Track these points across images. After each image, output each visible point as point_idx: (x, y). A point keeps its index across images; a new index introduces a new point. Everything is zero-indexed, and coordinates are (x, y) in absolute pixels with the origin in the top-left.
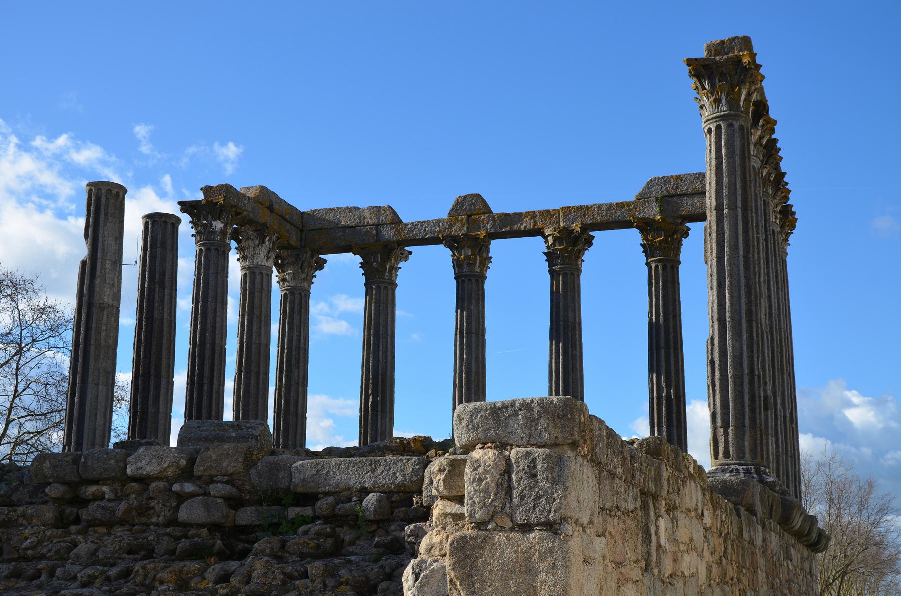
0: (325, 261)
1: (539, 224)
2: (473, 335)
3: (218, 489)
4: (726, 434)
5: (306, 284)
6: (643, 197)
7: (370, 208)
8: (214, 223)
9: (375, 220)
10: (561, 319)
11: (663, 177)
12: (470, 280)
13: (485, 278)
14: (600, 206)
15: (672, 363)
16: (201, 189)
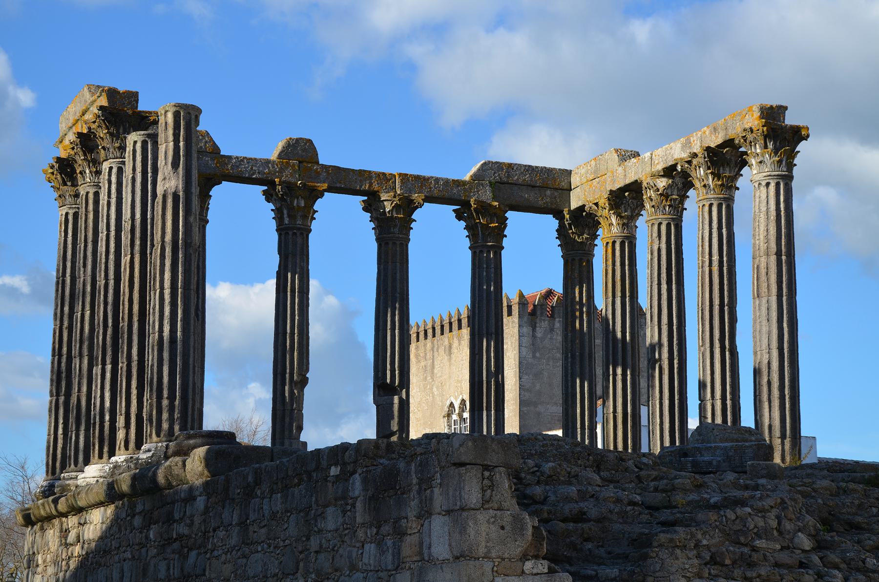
1: (376, 187)
4: (783, 444)
6: (476, 177)
10: (398, 290)
11: (497, 163)
14: (437, 180)
16: (112, 93)
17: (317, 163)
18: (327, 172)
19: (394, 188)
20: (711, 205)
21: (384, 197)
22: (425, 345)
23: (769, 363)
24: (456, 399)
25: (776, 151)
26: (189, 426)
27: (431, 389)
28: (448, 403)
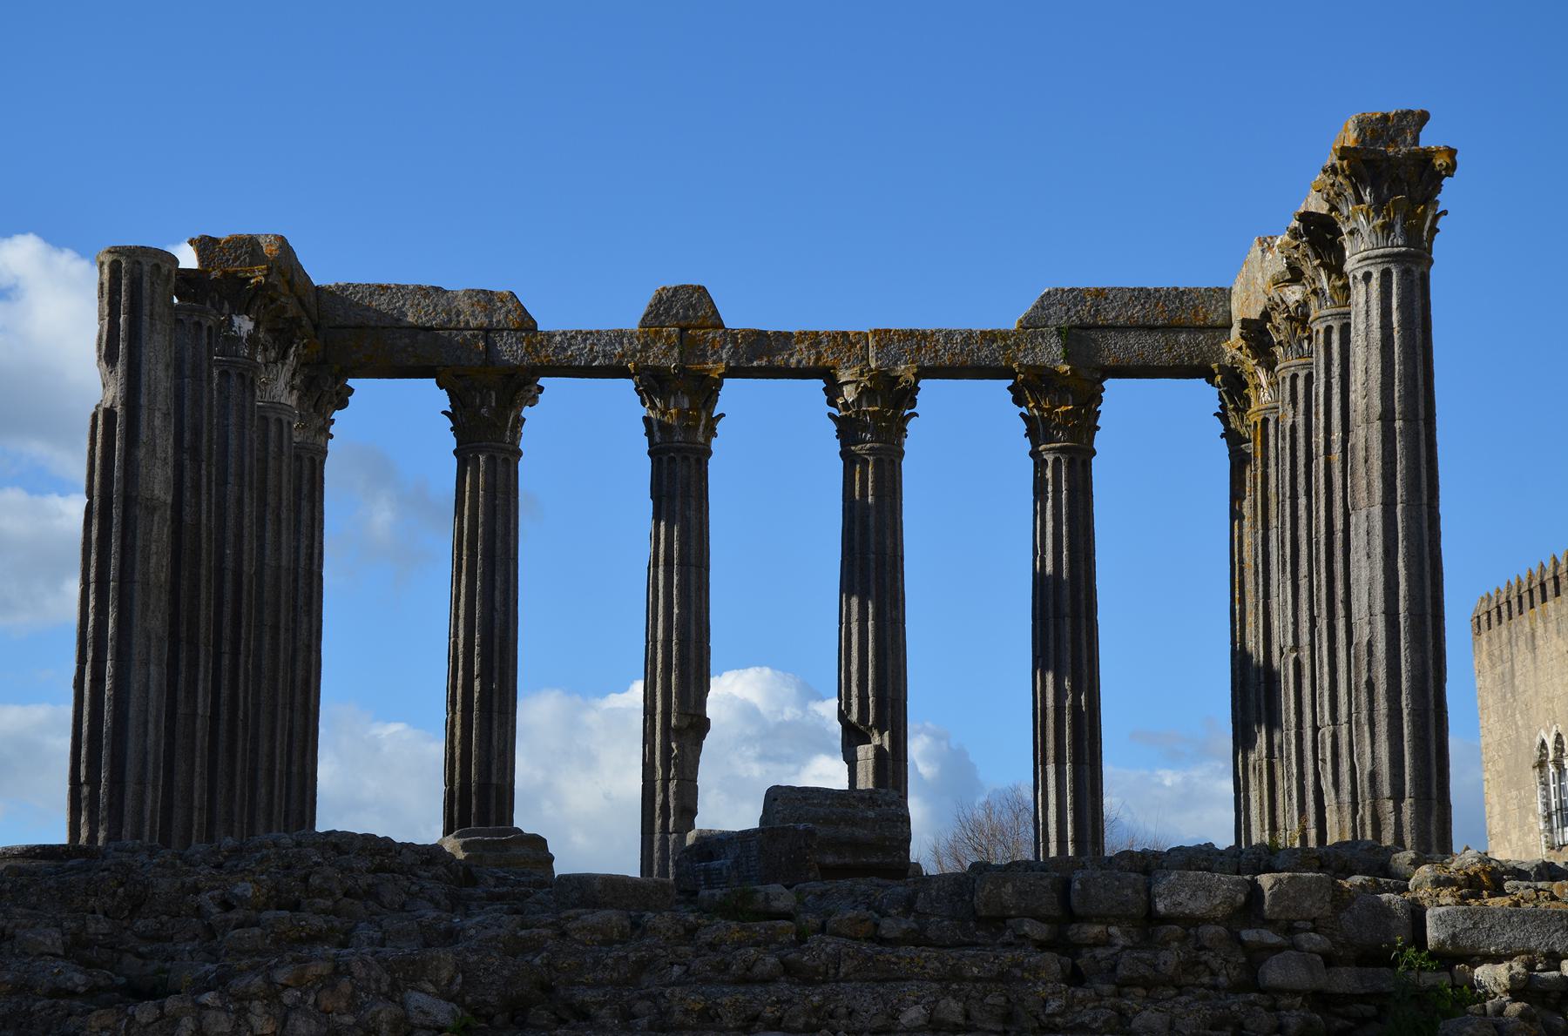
0: (351, 391)
1: (828, 359)
2: (693, 569)
3: (1314, 940)
4: (1398, 810)
5: (320, 439)
6: (1032, 324)
7: (470, 293)
8: (237, 320)
9: (482, 320)
10: (873, 548)
11: (1072, 290)
12: (686, 458)
13: (709, 453)
14: (949, 335)
15: (1051, 636)
17: (719, 325)
18: (735, 341)
19: (865, 358)
20: (1329, 330)
21: (844, 376)
22: (1500, 635)
23: (1370, 644)
24: (1548, 732)
25: (1379, 206)
26: (493, 817)
27: (1513, 715)
28: (1538, 741)
